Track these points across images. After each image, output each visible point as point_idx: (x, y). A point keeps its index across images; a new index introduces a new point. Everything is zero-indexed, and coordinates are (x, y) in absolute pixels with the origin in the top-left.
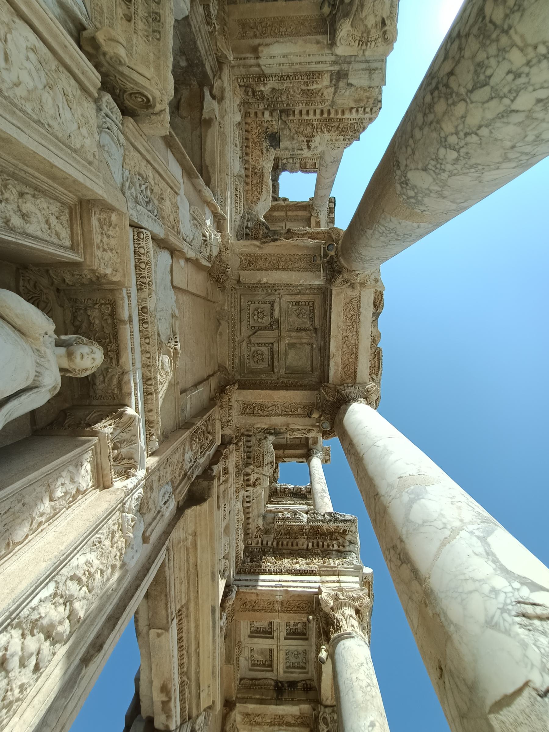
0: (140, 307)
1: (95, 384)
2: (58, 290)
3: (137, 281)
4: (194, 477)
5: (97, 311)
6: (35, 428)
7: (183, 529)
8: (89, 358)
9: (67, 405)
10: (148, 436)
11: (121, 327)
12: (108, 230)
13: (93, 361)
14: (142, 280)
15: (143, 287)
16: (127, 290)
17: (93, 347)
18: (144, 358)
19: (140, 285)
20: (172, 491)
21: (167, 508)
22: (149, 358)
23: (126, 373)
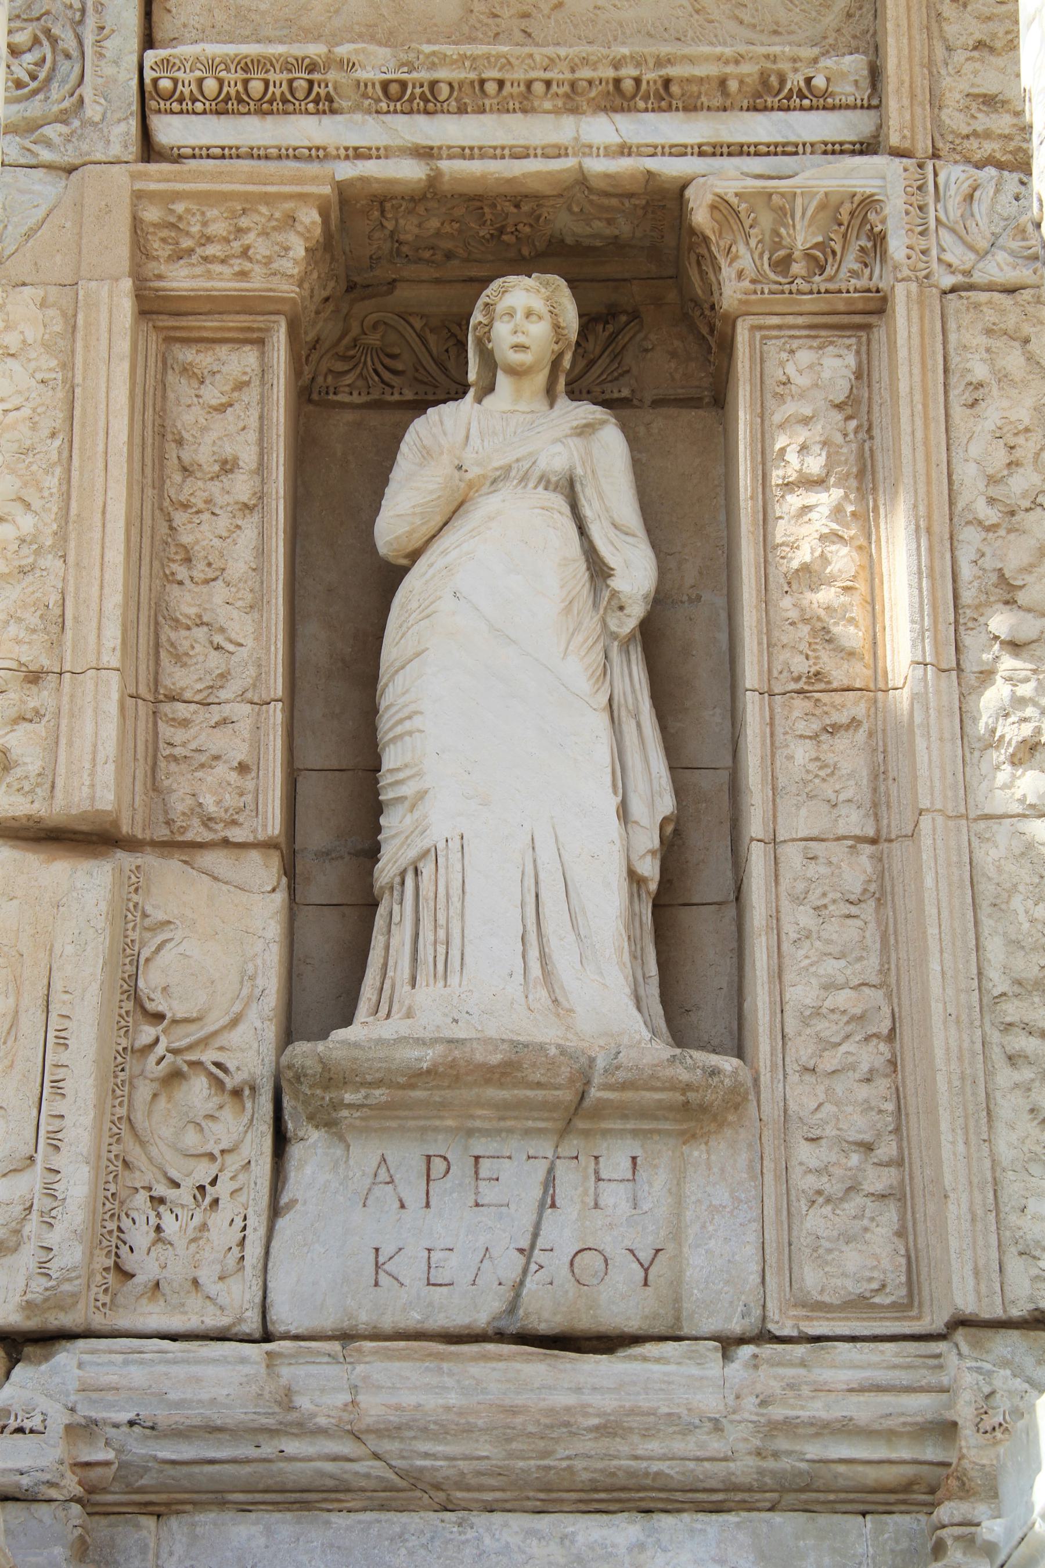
0: (383, 105)
1: (616, 237)
2: (351, 287)
3: (307, 112)
5: (402, 222)
6: (707, 400)
8: (526, 313)
9: (672, 296)
10: (806, 102)
11: (446, 187)
12: (188, 234)
13: (534, 318)
14: (300, 95)
15: (323, 92)
16: (338, 157)
17: (501, 307)
19: (317, 101)
22: (548, 83)
23: (585, 178)
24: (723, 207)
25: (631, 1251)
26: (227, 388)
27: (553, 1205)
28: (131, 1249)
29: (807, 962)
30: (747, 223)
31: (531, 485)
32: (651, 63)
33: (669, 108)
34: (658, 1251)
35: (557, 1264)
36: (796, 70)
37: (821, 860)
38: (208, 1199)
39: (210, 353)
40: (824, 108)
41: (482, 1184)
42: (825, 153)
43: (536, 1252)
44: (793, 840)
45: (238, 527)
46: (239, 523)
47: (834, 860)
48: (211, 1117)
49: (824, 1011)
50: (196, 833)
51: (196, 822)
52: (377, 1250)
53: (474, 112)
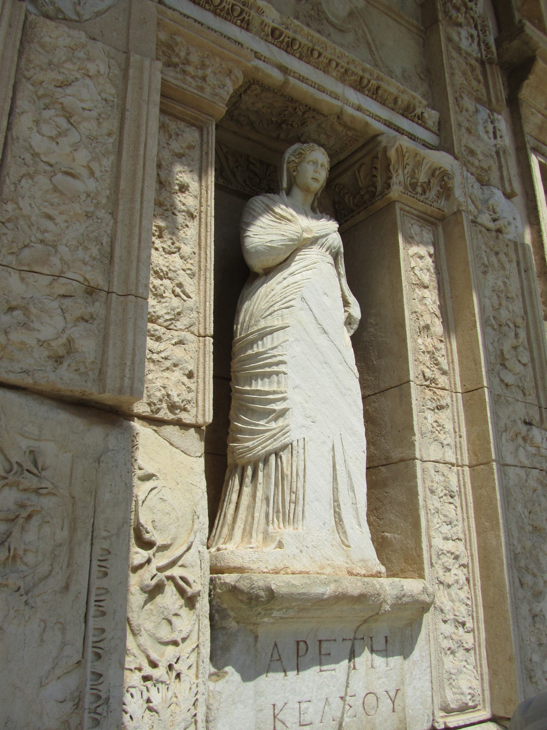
3: (235, 24)
4: (494, 49)
7: (533, 114)
10: (420, 122)
12: (178, 55)
18: (334, 74)
19: (242, 20)
20: (488, 111)
21: (501, 137)
22: (337, 65)
24: (400, 150)
25: (387, 692)
26: (184, 145)
27: (354, 668)
28: (131, 717)
29: (438, 525)
30: (405, 163)
31: (324, 249)
32: (375, 76)
33: (375, 99)
34: (397, 690)
35: (357, 702)
36: (419, 107)
37: (441, 473)
38: (174, 674)
39: (174, 123)
40: (424, 127)
41: (323, 657)
42: (423, 145)
43: (348, 698)
44: (430, 461)
45: (187, 226)
46: (188, 224)
47: (445, 474)
48: (176, 615)
49: (445, 552)
50: (164, 414)
51: (164, 405)
52: (274, 705)
53: (304, 61)
